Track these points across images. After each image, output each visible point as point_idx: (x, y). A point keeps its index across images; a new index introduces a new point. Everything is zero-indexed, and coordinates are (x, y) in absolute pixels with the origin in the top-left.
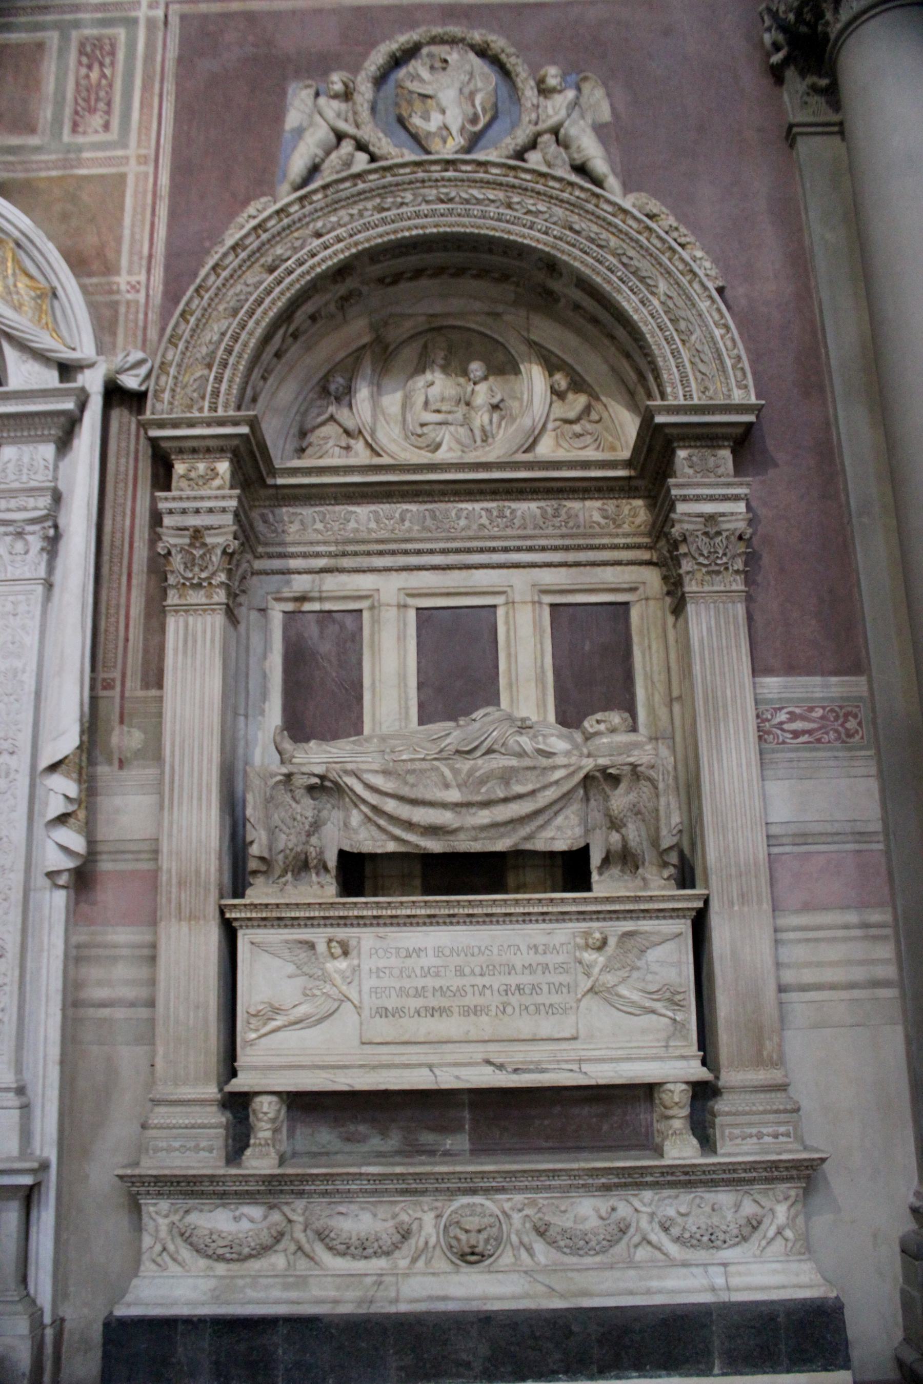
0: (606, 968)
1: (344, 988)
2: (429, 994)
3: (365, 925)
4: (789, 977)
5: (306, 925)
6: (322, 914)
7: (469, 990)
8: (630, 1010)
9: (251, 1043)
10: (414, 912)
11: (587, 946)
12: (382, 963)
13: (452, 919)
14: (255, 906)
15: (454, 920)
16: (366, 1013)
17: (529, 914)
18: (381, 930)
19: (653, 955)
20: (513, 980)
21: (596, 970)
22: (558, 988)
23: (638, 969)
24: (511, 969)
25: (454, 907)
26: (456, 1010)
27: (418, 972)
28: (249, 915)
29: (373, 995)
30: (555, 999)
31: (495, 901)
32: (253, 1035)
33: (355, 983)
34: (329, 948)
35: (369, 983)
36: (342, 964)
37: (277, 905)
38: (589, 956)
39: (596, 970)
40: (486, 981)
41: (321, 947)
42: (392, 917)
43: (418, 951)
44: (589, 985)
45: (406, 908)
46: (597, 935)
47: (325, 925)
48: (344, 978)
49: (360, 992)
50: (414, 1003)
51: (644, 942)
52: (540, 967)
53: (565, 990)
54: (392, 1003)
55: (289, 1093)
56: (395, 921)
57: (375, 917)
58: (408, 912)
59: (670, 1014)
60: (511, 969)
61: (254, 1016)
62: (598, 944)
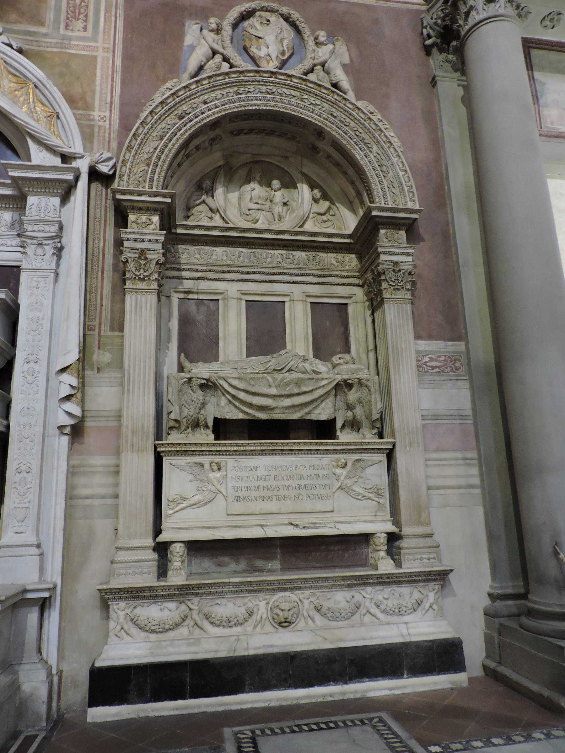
0: (347, 477)
1: (219, 487)
2: (261, 489)
3: (229, 455)
4: (432, 482)
5: (199, 455)
6: (208, 449)
7: (281, 487)
8: (358, 497)
9: (169, 516)
10: (254, 449)
11: (338, 465)
12: (238, 474)
13: (272, 452)
14: (174, 444)
15: (274, 453)
16: (229, 499)
17: (310, 450)
18: (237, 457)
19: (369, 471)
20: (302, 483)
21: (342, 478)
22: (324, 486)
23: (362, 477)
24: (301, 477)
25: (274, 446)
26: (274, 498)
27: (256, 478)
28: (170, 449)
29: (233, 490)
30: (323, 492)
31: (294, 443)
32: (171, 512)
33: (224, 485)
34: (211, 466)
35: (231, 484)
36: (218, 475)
37: (185, 444)
38: (338, 471)
39: (342, 478)
40: (290, 483)
41: (207, 466)
42: (243, 451)
43: (256, 468)
44: (339, 485)
45: (251, 446)
46: (343, 461)
47: (209, 455)
48: (219, 481)
49: (227, 488)
50: (254, 494)
51: (365, 465)
52: (315, 476)
53: (327, 487)
54: (242, 494)
55: (188, 542)
56: (244, 453)
57: (234, 451)
58: (252, 448)
59: (377, 499)
60: (301, 477)
61: (171, 501)
62: (343, 465)
